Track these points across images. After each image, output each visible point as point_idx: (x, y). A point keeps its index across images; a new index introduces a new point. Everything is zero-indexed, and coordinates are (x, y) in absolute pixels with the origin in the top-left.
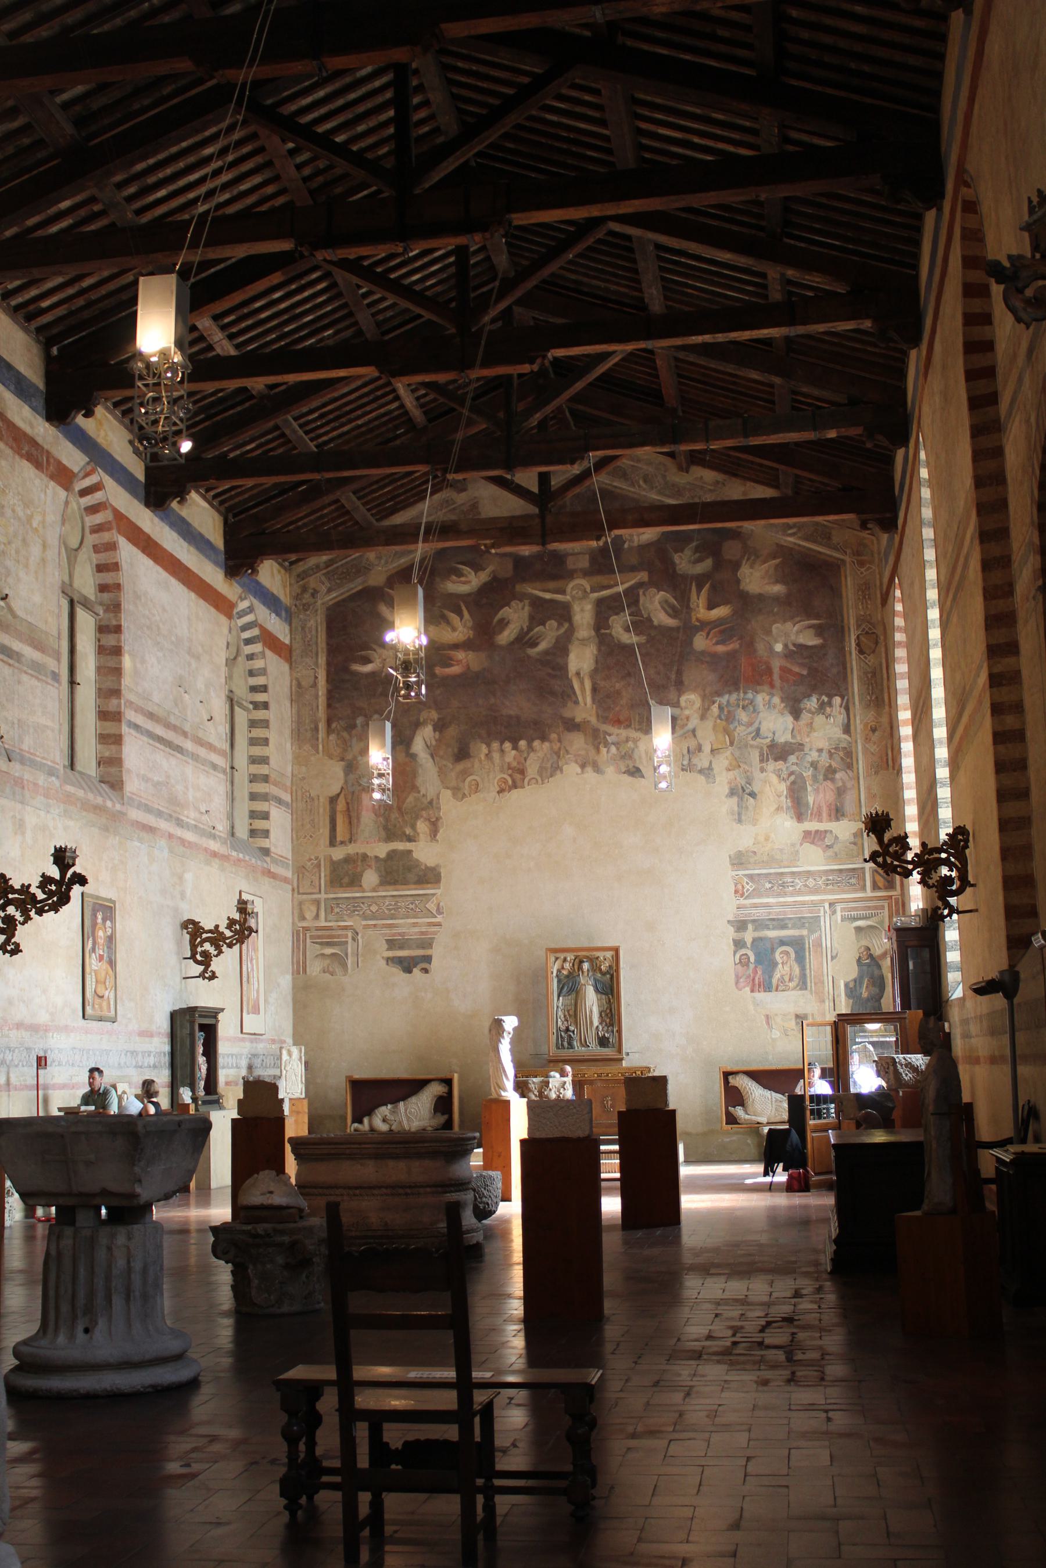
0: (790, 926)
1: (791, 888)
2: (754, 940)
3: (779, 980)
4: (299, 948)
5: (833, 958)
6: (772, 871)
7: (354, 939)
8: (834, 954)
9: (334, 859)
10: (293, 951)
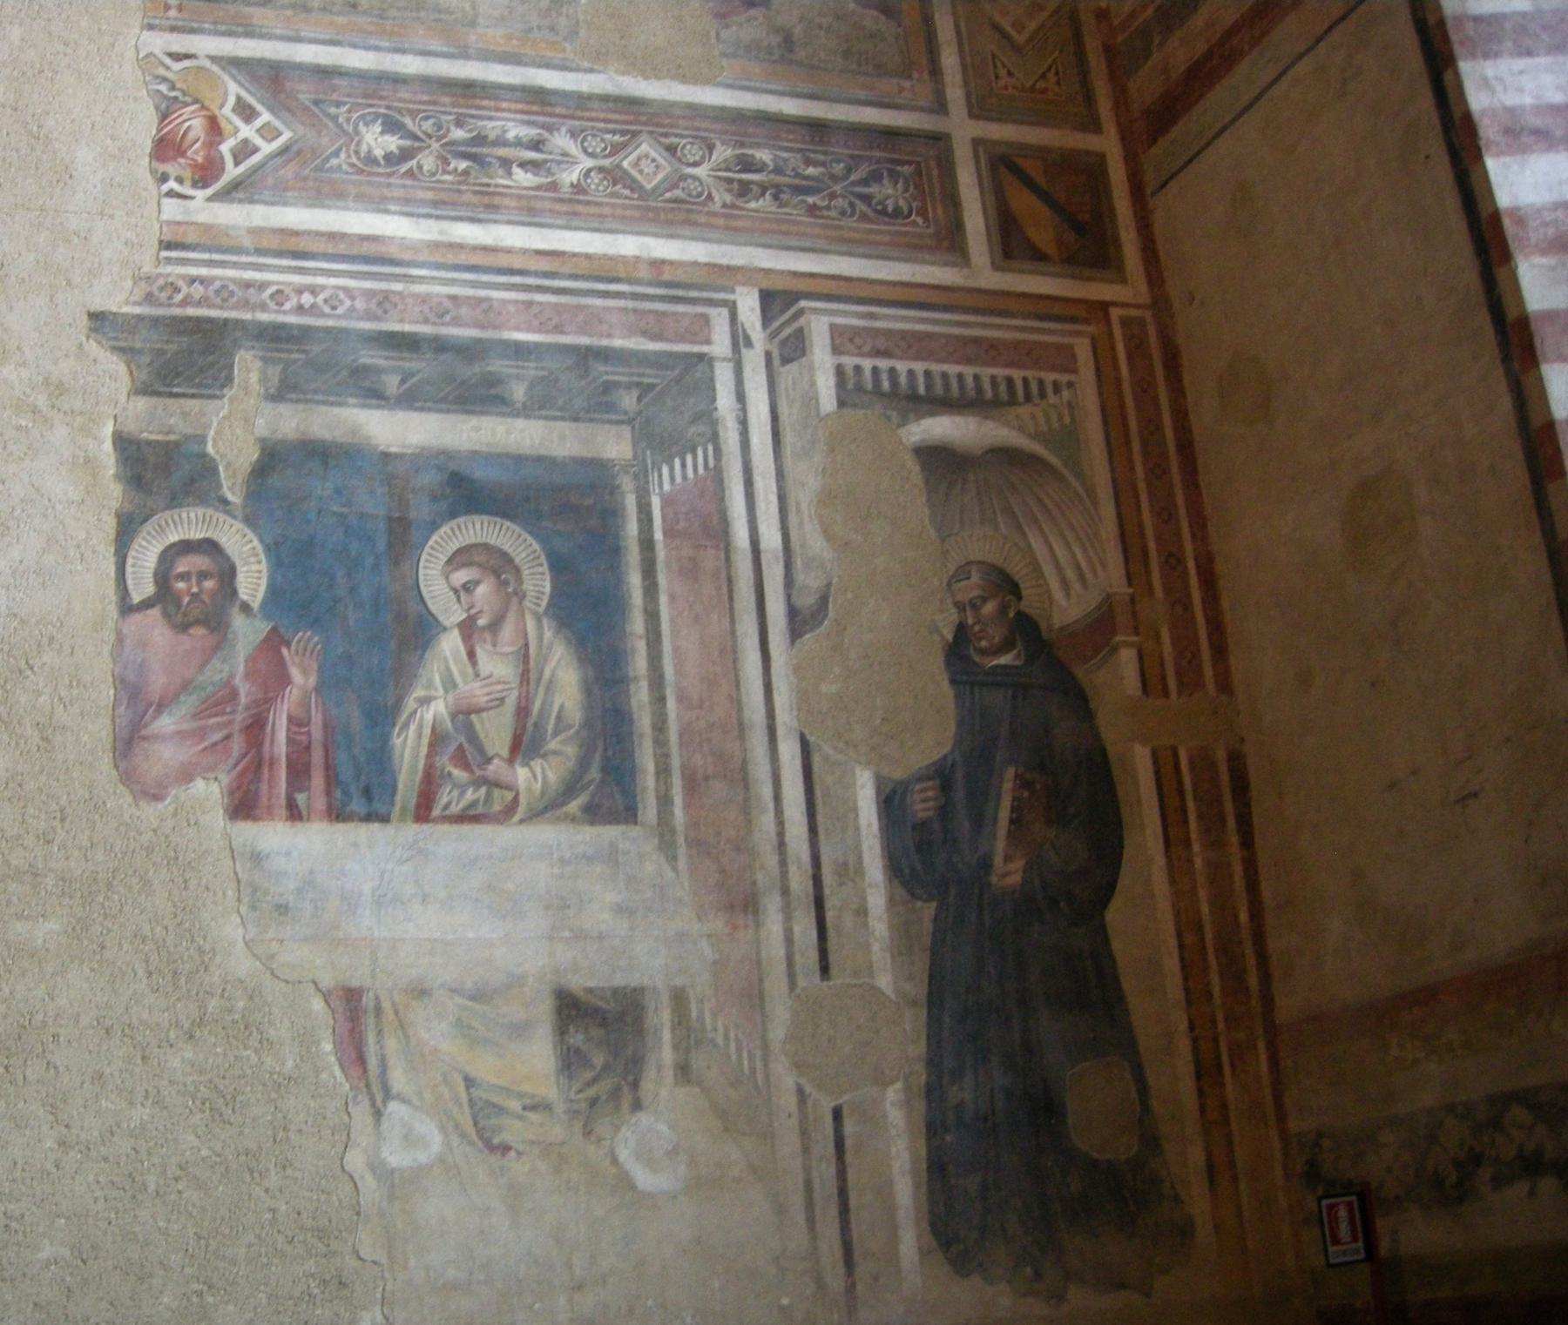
0: (519, 392)
1: (522, 177)
2: (272, 458)
3: (438, 739)
5: (798, 622)
6: (411, 65)
8: (806, 601)
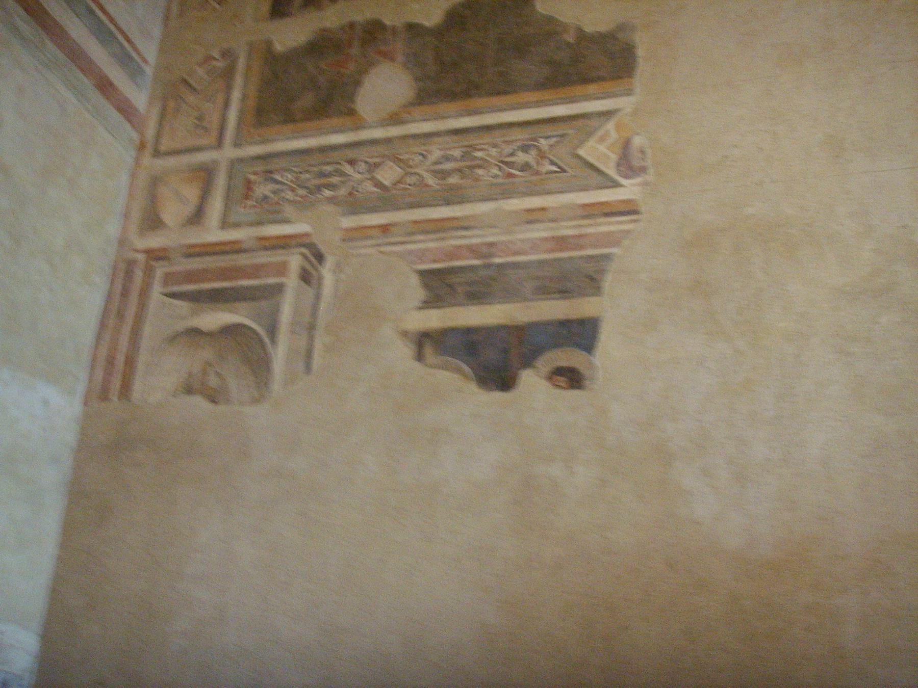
4: (121, 316)
7: (305, 277)
9: (279, 48)
10: (103, 325)
